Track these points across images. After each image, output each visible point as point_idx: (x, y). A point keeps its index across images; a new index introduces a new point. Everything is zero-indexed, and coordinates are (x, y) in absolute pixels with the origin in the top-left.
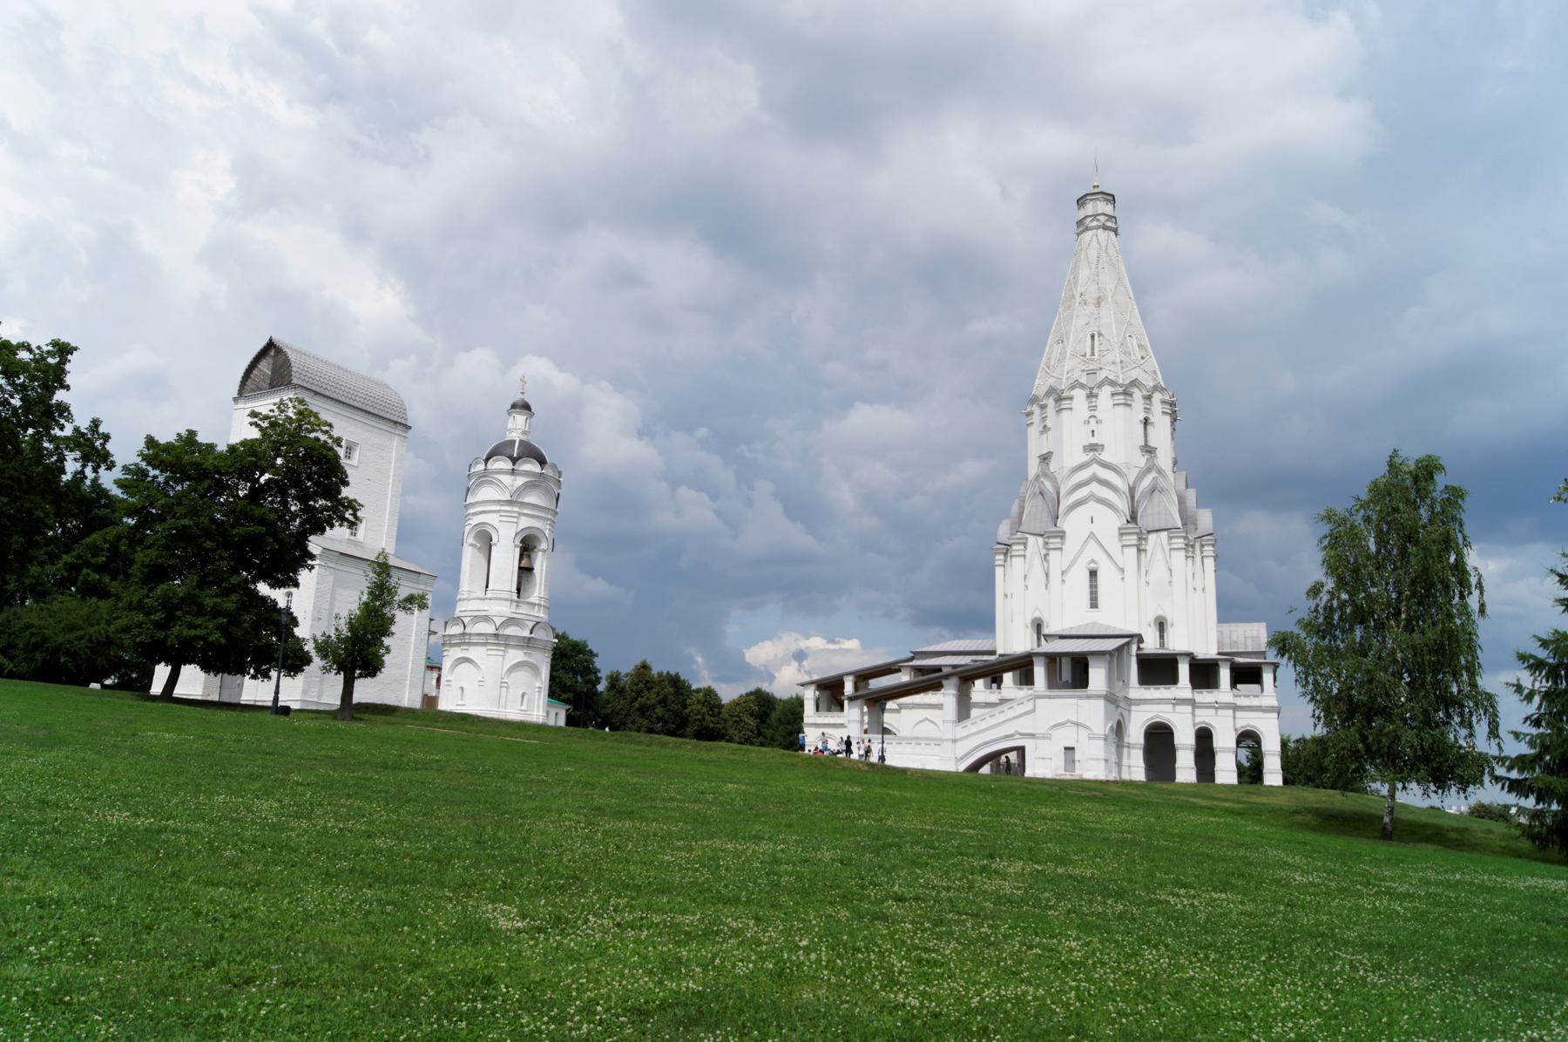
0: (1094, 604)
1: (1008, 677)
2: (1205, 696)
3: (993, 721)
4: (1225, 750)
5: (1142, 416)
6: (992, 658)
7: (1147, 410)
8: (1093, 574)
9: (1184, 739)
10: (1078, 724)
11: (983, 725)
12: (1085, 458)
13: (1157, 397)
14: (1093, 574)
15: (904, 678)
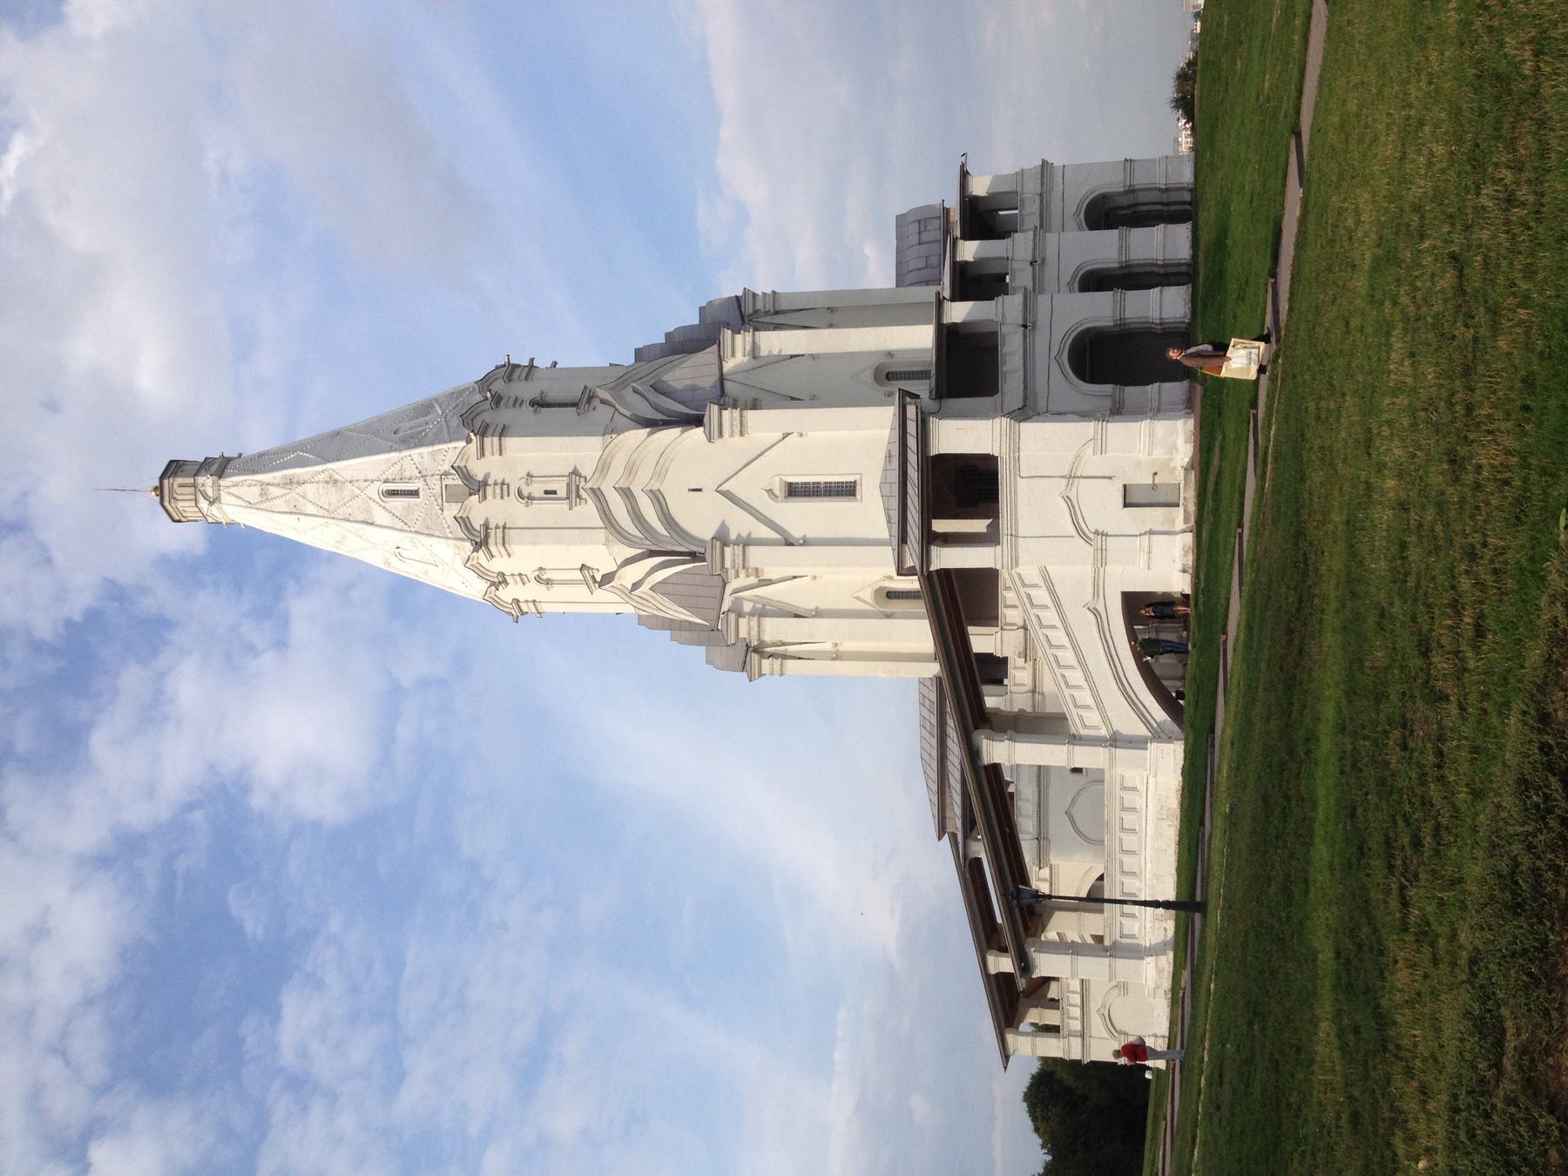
0: (847, 490)
1: (982, 641)
2: (1020, 277)
3: (1068, 656)
4: (1124, 246)
5: (527, 411)
6: (946, 683)
7: (517, 402)
8: (795, 491)
9: (1100, 309)
10: (1071, 477)
11: (1076, 677)
12: (588, 511)
13: (498, 386)
14: (795, 491)
15: (980, 850)
